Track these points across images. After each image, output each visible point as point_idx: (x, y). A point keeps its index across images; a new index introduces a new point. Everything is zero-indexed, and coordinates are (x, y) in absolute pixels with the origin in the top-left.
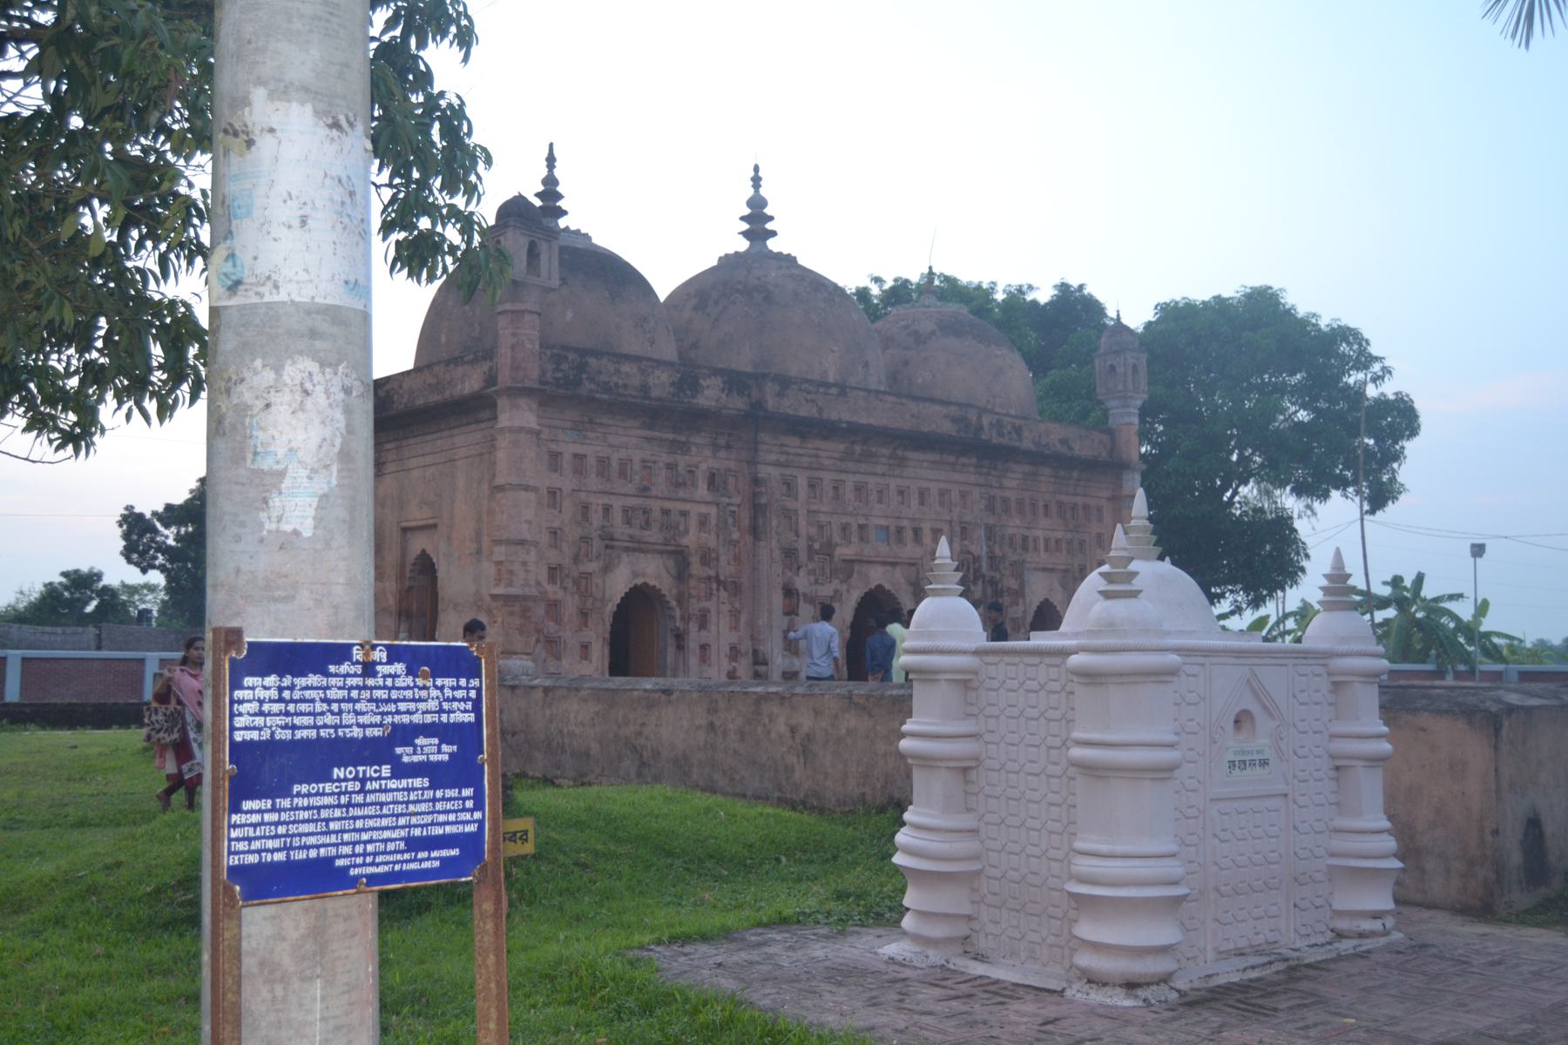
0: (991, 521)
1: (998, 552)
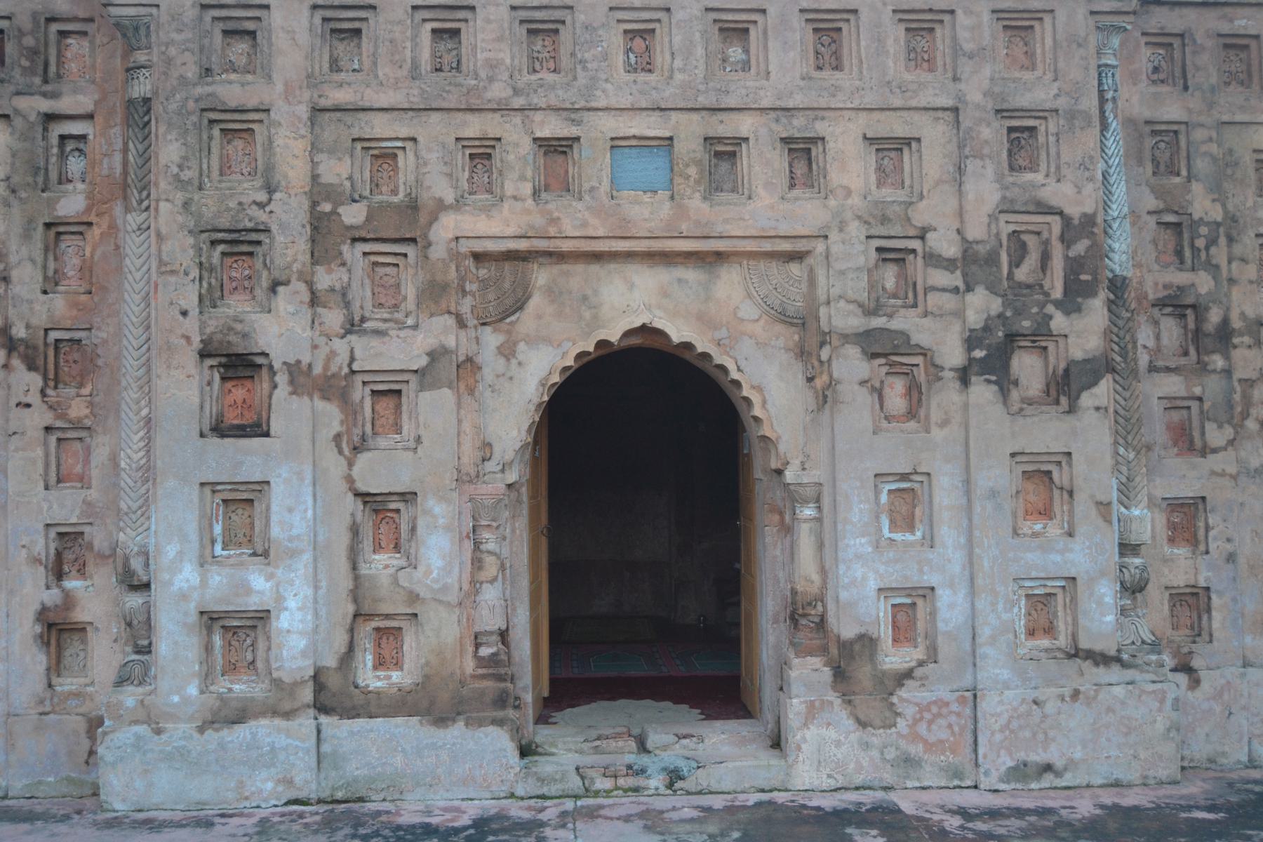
0: (1172, 110)
1: (1202, 205)
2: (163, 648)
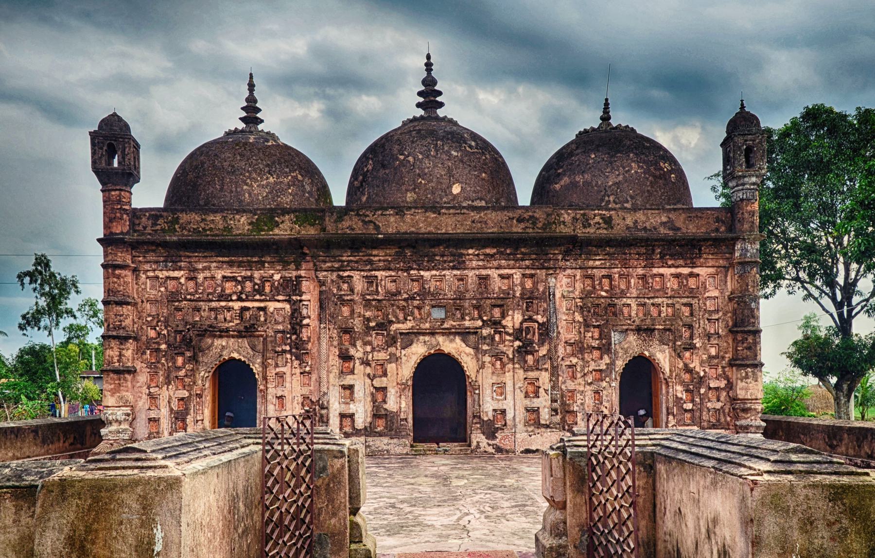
2: (331, 421)
